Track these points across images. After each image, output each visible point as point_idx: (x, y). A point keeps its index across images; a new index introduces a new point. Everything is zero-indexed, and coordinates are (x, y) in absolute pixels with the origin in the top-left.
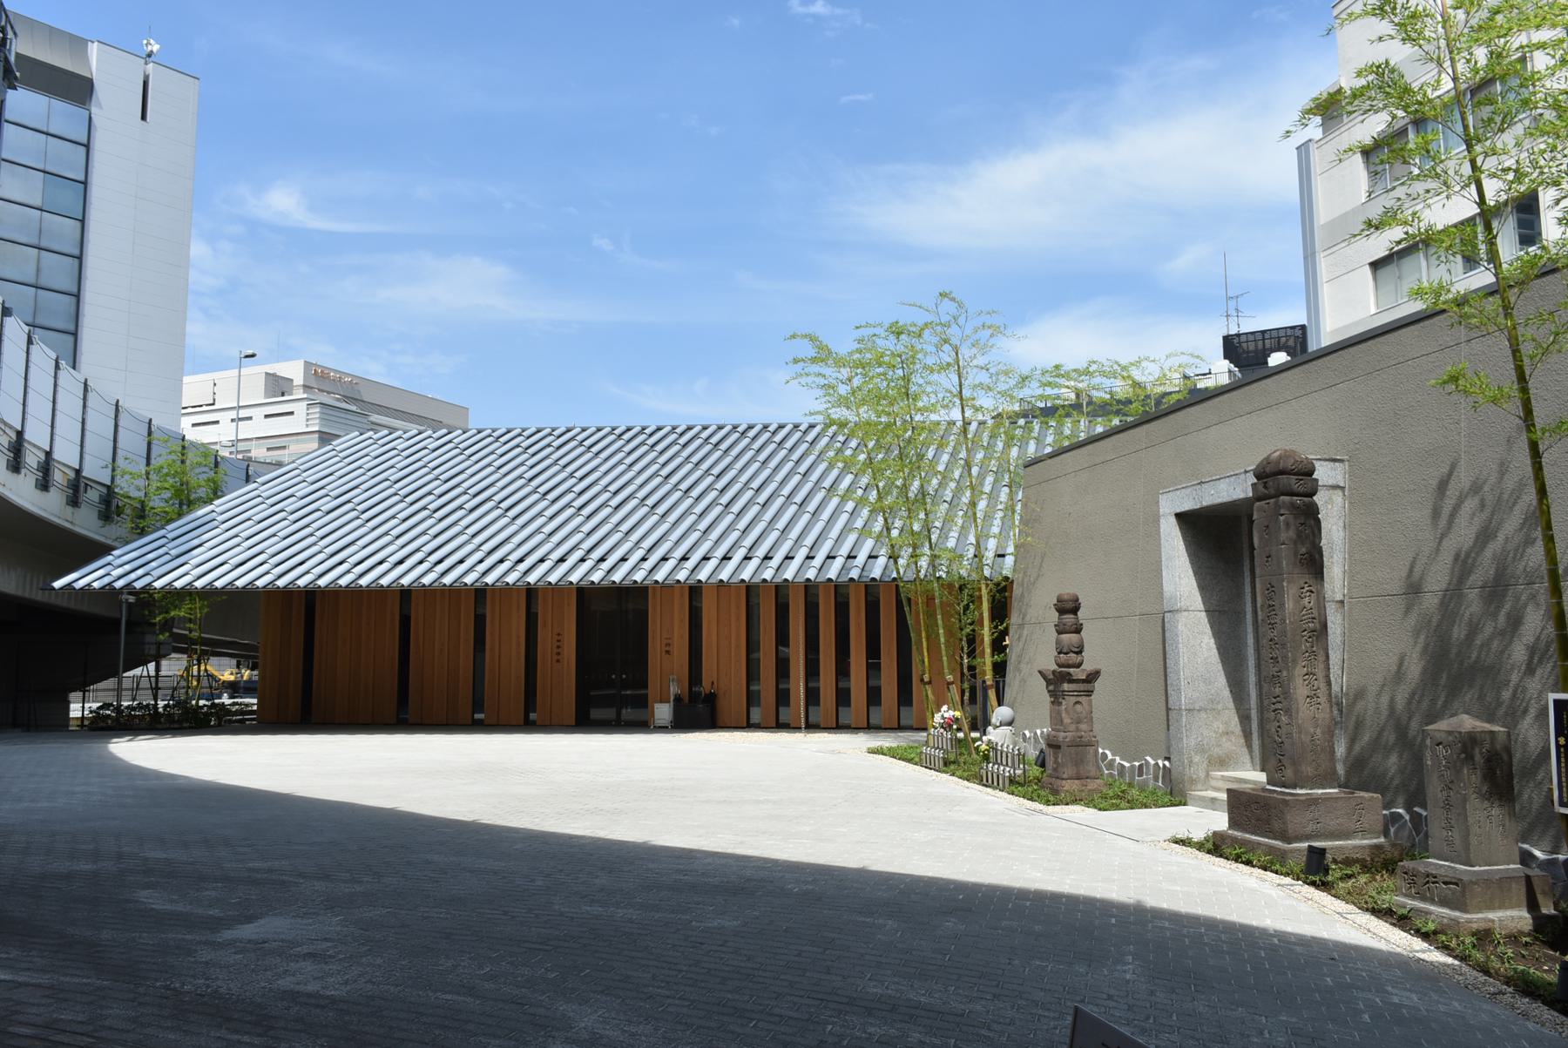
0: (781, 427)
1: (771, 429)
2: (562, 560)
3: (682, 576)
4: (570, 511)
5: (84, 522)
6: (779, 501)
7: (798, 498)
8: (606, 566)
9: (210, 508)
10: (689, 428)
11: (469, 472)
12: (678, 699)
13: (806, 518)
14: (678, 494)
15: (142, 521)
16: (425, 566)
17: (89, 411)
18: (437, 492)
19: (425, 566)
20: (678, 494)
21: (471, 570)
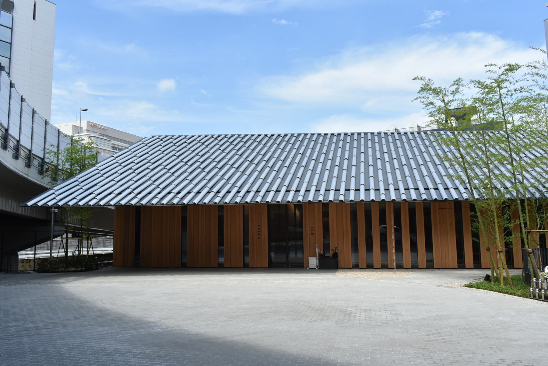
0: (233, 136)
1: (242, 136)
2: (199, 192)
3: (217, 200)
4: (199, 170)
5: (32, 175)
6: (295, 166)
7: (236, 165)
8: (180, 196)
9: (95, 168)
10: (193, 136)
11: (150, 153)
12: (320, 256)
13: (239, 174)
14: (247, 163)
15: (56, 175)
16: (132, 195)
17: (35, 123)
18: (136, 162)
19: (132, 195)
20: (247, 163)
21: (155, 197)
